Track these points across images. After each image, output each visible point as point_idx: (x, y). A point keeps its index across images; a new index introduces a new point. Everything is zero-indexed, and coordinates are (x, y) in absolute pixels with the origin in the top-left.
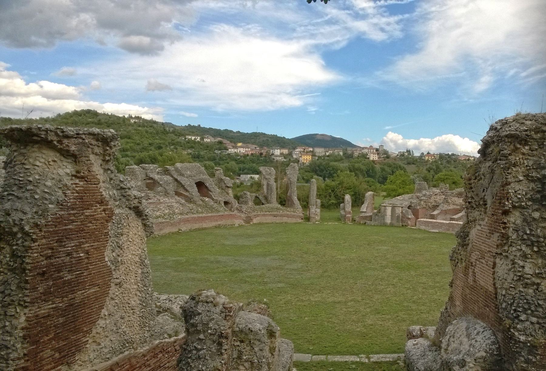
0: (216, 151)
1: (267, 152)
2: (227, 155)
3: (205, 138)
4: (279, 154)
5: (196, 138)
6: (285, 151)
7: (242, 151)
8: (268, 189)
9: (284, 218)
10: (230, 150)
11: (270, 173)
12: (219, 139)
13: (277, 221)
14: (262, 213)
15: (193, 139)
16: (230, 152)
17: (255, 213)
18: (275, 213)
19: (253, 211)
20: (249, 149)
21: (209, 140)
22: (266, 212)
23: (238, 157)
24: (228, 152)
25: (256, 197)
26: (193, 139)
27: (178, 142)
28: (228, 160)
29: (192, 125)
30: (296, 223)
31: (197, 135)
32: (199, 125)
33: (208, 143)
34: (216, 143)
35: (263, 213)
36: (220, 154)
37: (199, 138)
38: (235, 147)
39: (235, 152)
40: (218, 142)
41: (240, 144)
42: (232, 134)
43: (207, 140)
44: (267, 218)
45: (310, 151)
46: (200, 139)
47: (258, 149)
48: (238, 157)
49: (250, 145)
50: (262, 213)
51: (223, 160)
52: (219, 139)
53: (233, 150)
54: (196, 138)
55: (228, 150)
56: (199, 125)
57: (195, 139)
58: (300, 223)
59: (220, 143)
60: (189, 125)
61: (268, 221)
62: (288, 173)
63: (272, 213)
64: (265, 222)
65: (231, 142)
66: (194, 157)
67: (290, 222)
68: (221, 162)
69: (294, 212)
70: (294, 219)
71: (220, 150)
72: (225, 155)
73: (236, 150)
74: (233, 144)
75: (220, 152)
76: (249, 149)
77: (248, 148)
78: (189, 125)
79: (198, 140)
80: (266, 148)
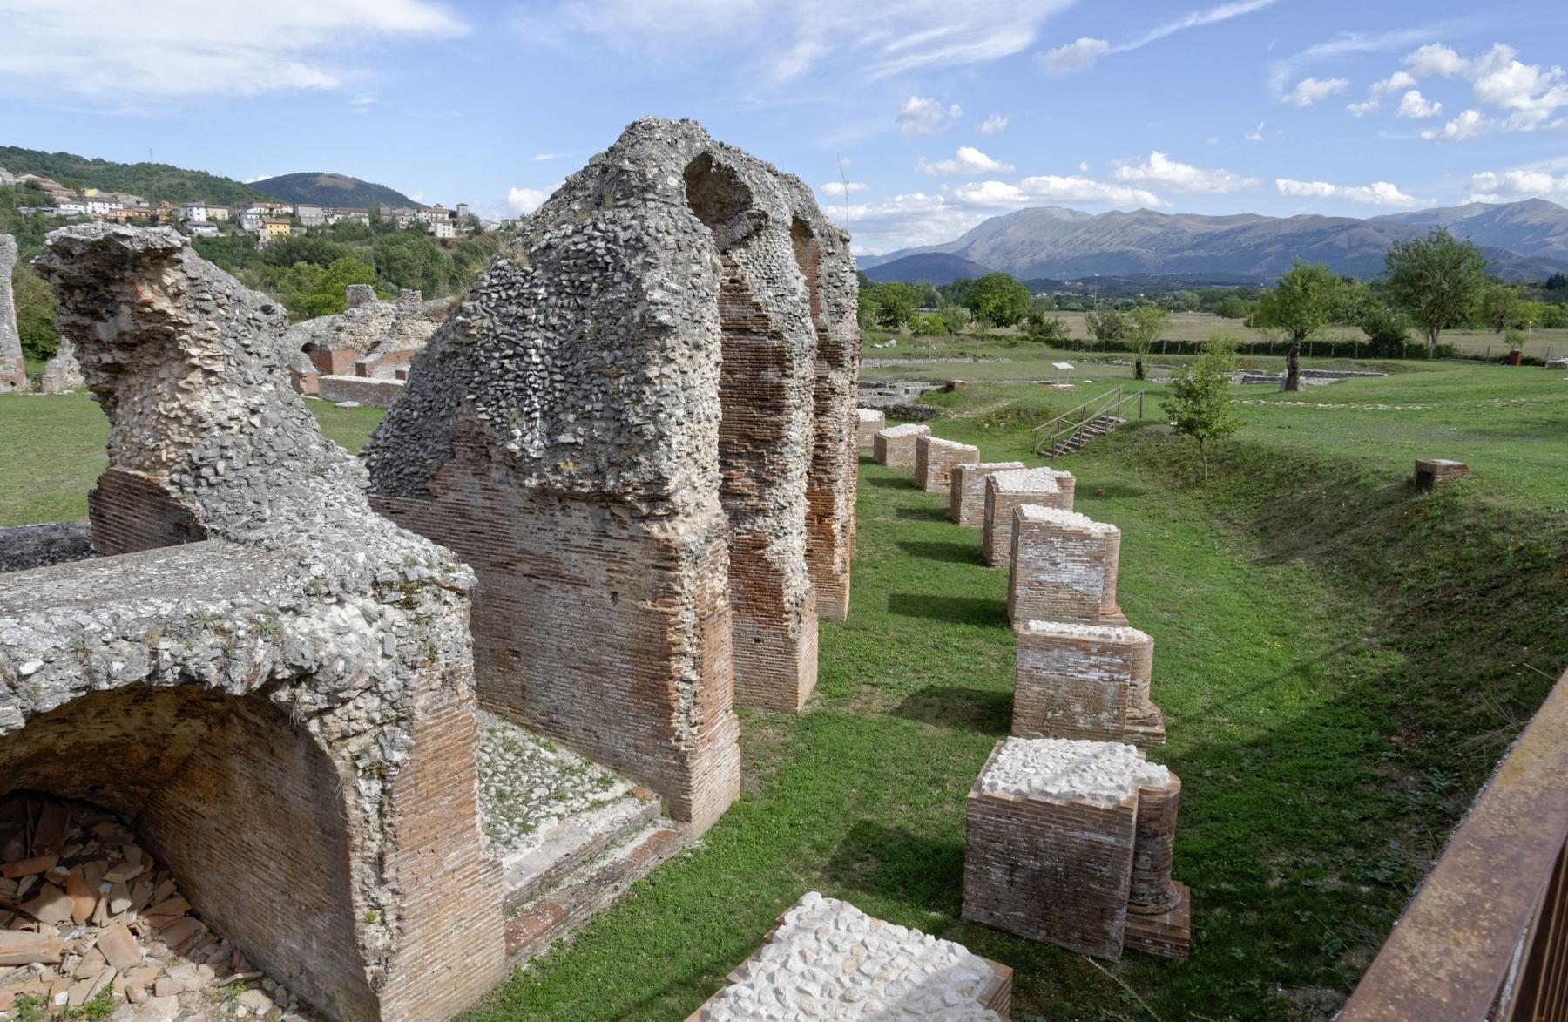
0: (23, 210)
1: (170, 214)
4: (203, 219)
6: (222, 213)
7: (101, 209)
10: (63, 207)
12: (30, 176)
16: (63, 213)
20: (121, 207)
24: (56, 212)
38: (83, 200)
39: (80, 213)
41: (91, 193)
45: (287, 214)
47: (147, 205)
49: (121, 196)
52: (30, 176)
53: (72, 207)
55: (56, 206)
59: (32, 186)
65: (66, 185)
72: (50, 219)
74: (73, 193)
75: (33, 210)
76: (121, 207)
77: (117, 202)
80: (167, 204)
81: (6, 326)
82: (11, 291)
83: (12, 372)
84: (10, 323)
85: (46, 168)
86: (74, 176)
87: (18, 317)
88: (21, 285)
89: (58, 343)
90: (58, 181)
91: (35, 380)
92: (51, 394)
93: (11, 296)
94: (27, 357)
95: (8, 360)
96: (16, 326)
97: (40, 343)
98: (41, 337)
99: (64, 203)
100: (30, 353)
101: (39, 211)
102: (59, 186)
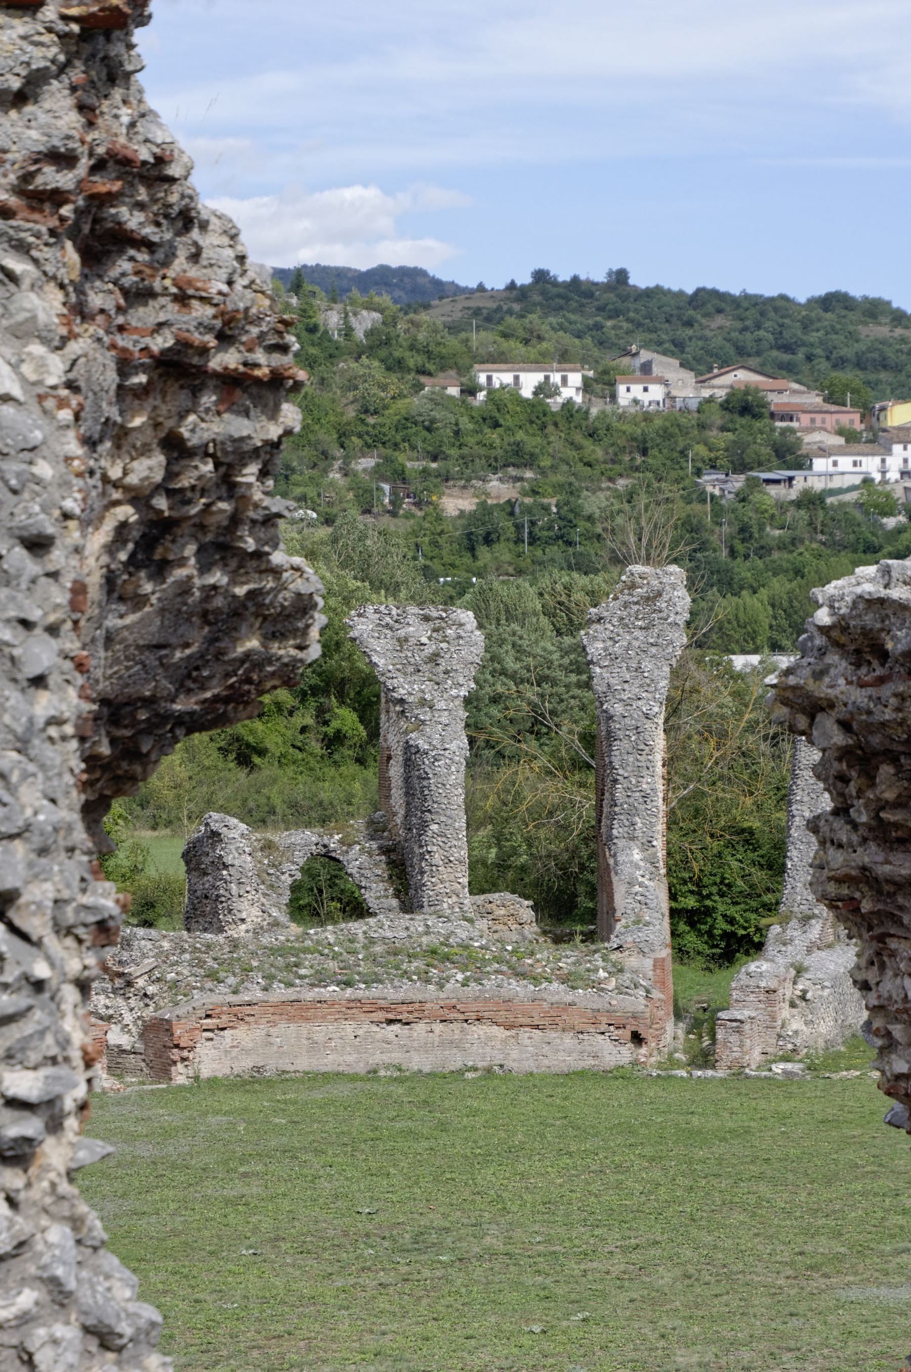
0: (711, 484)
2: (798, 504)
3: (628, 375)
5: (556, 378)
8: (409, 792)
9: (478, 1031)
10: (820, 464)
11: (434, 659)
12: (741, 377)
13: (418, 1062)
14: (280, 992)
15: (527, 393)
16: (818, 485)
17: (221, 996)
18: (407, 990)
19: (212, 975)
21: (656, 392)
22: (320, 979)
23: (891, 522)
25: (328, 857)
26: (527, 393)
27: (408, 420)
28: (805, 554)
29: (564, 275)
30: (581, 1074)
31: (564, 358)
32: (621, 276)
33: (647, 417)
34: (717, 418)
35: (290, 994)
36: (742, 497)
37: (575, 379)
39: (867, 481)
40: (726, 406)
42: (881, 331)
43: (637, 390)
44: (320, 1031)
46: (587, 387)
48: (891, 522)
50: (280, 992)
51: (763, 551)
52: (741, 377)
53: (845, 463)
54: (556, 378)
55: (802, 463)
56: (621, 276)
57: (544, 389)
58: (618, 1074)
60: (541, 276)
61: (328, 1062)
62: (595, 649)
63: (376, 991)
64: (303, 1063)
65: (834, 398)
66: (533, 540)
67: (530, 1065)
68: (743, 570)
69: (569, 980)
70: (568, 1040)
71: (741, 467)
72: (782, 506)
73: (871, 465)
74: (852, 419)
75: (738, 482)
78: (541, 276)
79: (568, 393)
81: (637, 855)
82: (660, 741)
83: (637, 1002)
84: (648, 844)
85: (787, 348)
86: (860, 364)
87: (672, 823)
88: (689, 723)
89: (771, 908)
90: (815, 383)
91: (695, 1026)
92: (738, 1073)
93: (659, 757)
94: (681, 953)
95: (632, 961)
96: (661, 854)
97: (722, 906)
98: (725, 888)
99: (824, 452)
100: (691, 940)
101: (753, 484)
102: (814, 399)
